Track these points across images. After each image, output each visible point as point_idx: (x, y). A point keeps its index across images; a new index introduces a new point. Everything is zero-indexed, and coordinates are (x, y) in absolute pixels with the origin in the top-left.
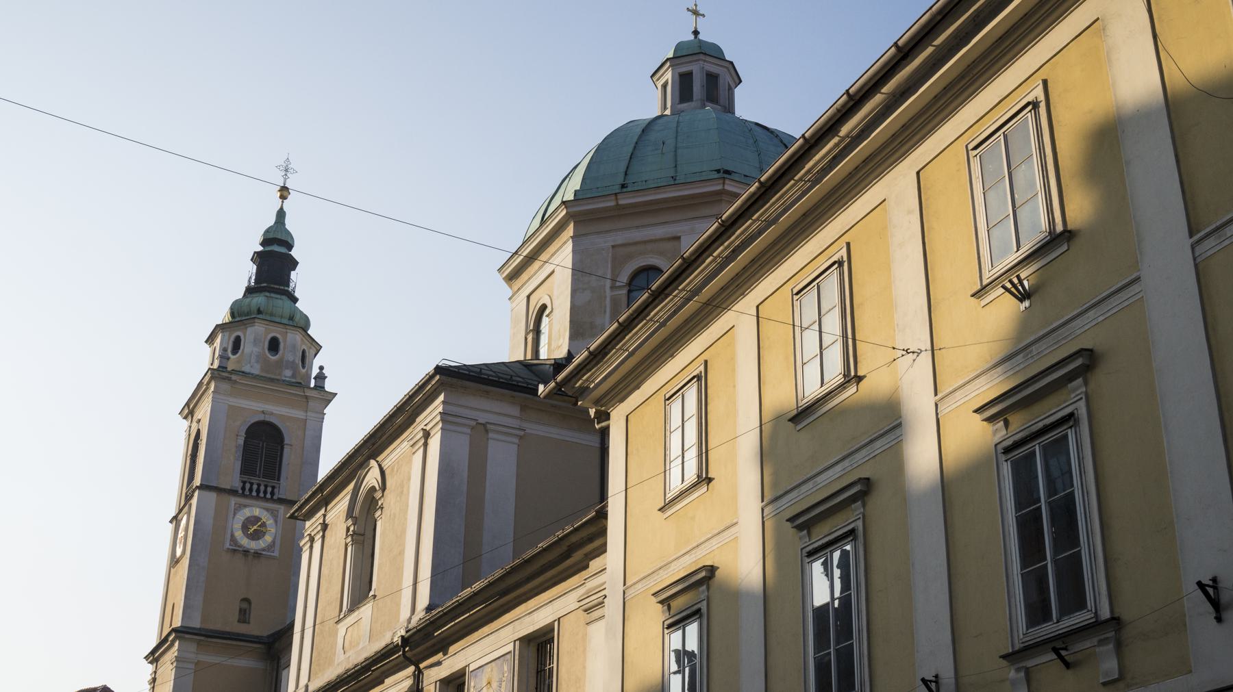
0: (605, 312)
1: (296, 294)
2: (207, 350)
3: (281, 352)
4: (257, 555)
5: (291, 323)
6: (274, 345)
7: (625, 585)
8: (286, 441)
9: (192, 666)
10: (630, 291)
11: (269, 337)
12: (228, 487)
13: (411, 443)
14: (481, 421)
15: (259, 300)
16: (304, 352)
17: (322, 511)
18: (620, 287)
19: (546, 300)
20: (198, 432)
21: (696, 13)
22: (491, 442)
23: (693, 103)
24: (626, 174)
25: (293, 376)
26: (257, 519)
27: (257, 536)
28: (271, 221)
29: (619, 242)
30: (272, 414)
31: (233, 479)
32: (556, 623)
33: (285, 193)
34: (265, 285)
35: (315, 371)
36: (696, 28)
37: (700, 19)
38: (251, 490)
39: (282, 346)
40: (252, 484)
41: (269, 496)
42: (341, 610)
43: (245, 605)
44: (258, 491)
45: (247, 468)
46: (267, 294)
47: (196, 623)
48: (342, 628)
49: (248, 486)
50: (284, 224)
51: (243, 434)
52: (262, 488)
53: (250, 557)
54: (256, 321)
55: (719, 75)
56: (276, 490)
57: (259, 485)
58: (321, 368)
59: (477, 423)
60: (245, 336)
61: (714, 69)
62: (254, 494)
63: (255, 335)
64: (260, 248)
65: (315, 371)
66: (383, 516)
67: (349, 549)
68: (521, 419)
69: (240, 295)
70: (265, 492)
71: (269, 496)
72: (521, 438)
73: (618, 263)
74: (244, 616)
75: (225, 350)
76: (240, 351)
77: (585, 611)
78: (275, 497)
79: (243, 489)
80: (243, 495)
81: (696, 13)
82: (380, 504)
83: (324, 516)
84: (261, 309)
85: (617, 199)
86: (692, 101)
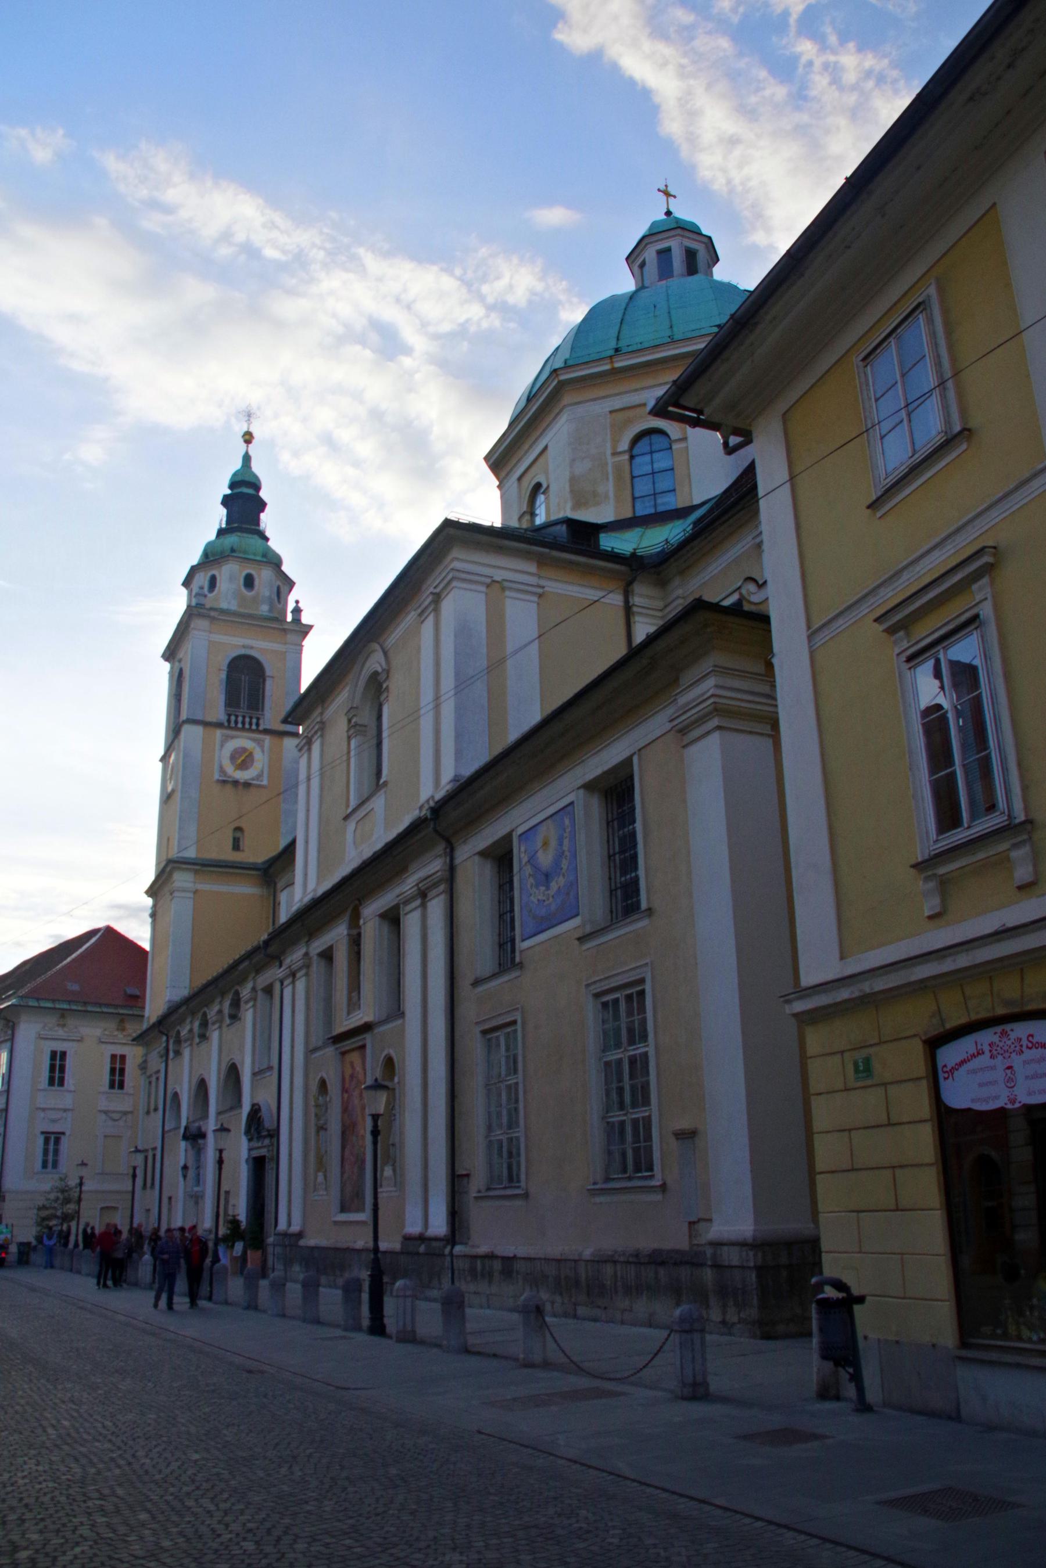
0: (607, 479)
1: (268, 534)
2: (184, 592)
3: (256, 588)
4: (247, 785)
5: (265, 560)
6: (249, 582)
7: (809, 627)
8: (268, 673)
9: (191, 895)
10: (632, 457)
11: (244, 574)
12: (214, 720)
13: (419, 611)
14: (497, 578)
15: (232, 540)
16: (278, 588)
17: (319, 710)
18: (624, 452)
19: (541, 478)
20: (181, 670)
21: (667, 194)
22: (508, 602)
23: (674, 279)
24: (618, 339)
25: (270, 611)
26: (244, 750)
27: (244, 766)
28: (237, 465)
29: (617, 407)
30: (252, 648)
31: (218, 713)
32: (635, 760)
33: (247, 437)
34: (236, 525)
35: (291, 606)
36: (668, 209)
37: (671, 199)
38: (236, 722)
39: (257, 582)
40: (237, 716)
41: (254, 727)
42: (348, 806)
43: (238, 834)
44: (243, 723)
45: (232, 700)
46: (239, 534)
47: (191, 853)
48: (351, 825)
49: (233, 718)
50: (250, 468)
51: (225, 668)
52: (247, 720)
53: (240, 787)
54: (230, 558)
55: (697, 250)
56: (261, 722)
57: (244, 717)
58: (297, 602)
59: (494, 581)
60: (220, 575)
61: (694, 245)
62: (240, 725)
63: (229, 574)
64: (229, 492)
65: (291, 606)
66: (390, 698)
67: (353, 743)
68: (540, 577)
69: (212, 536)
70: (251, 724)
71: (254, 727)
72: (540, 596)
73: (617, 430)
74: (236, 846)
75: (202, 588)
76: (217, 589)
77: (680, 731)
78: (261, 728)
79: (229, 721)
80: (229, 727)
81: (667, 194)
82: (384, 686)
83: (322, 714)
84: (235, 547)
85: (612, 362)
86: (672, 276)
